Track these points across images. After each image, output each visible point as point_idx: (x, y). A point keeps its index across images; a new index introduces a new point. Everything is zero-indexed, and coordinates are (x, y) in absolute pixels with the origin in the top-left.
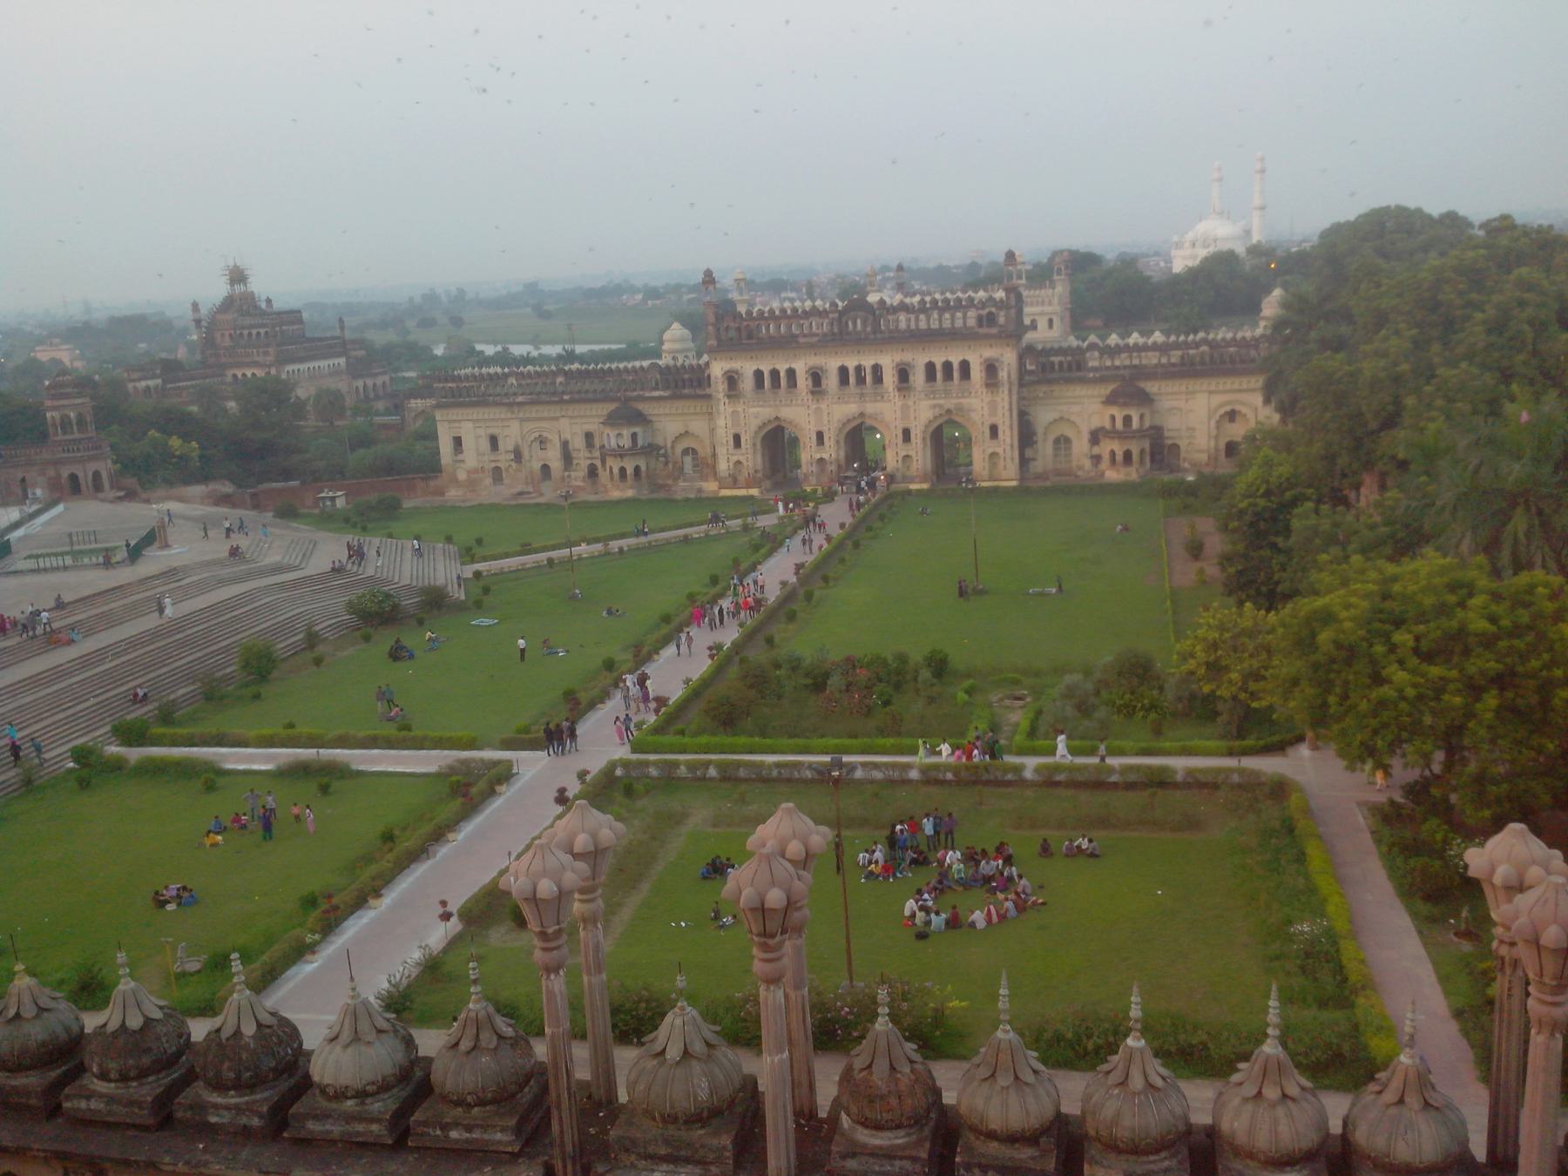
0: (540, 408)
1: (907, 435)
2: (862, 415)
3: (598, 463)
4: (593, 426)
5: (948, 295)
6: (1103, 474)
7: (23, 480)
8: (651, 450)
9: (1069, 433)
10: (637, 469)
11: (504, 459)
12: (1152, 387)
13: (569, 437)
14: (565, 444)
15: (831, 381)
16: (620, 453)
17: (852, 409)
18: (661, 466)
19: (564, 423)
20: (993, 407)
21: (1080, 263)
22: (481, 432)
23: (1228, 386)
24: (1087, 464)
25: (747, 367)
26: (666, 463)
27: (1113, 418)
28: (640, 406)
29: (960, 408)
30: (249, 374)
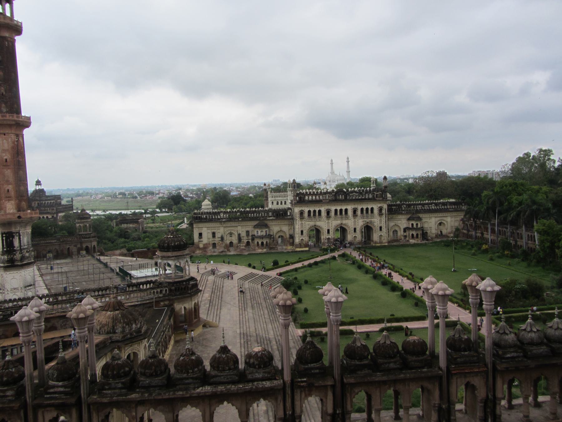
0: (231, 223)
1: (355, 229)
2: (342, 224)
3: (250, 241)
4: (250, 229)
5: (311, 191)
6: (408, 241)
7: (69, 248)
8: (269, 236)
9: (397, 229)
10: (267, 242)
11: (217, 240)
12: (421, 215)
13: (241, 232)
14: (239, 235)
15: (332, 214)
16: (262, 237)
17: (339, 222)
18: (272, 241)
19: (239, 228)
20: (381, 221)
21: (296, 185)
22: (210, 231)
23: (440, 215)
24: (403, 238)
25: (306, 209)
26: (274, 241)
27: (412, 224)
28: (266, 222)
29: (371, 222)
30: (45, 216)
